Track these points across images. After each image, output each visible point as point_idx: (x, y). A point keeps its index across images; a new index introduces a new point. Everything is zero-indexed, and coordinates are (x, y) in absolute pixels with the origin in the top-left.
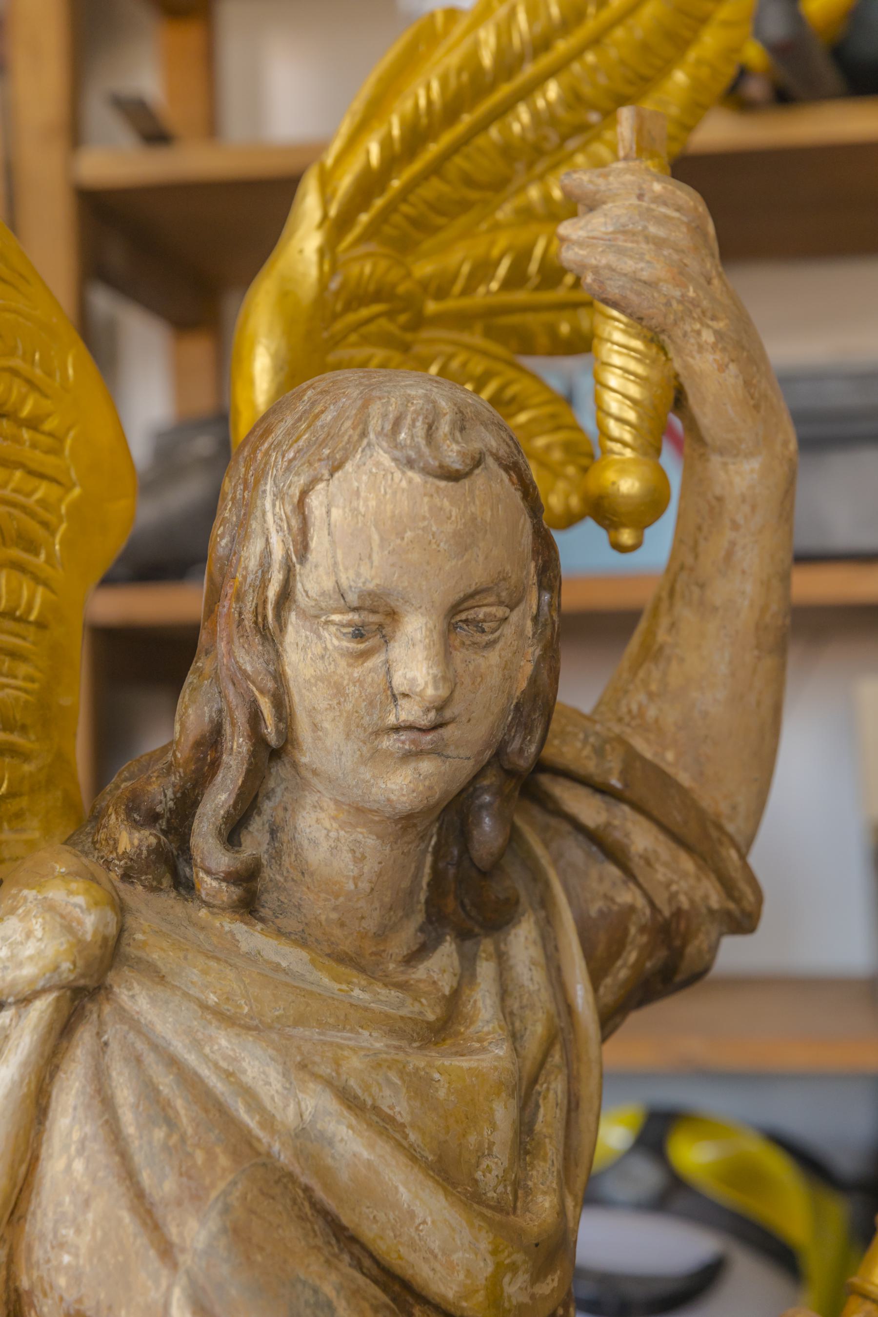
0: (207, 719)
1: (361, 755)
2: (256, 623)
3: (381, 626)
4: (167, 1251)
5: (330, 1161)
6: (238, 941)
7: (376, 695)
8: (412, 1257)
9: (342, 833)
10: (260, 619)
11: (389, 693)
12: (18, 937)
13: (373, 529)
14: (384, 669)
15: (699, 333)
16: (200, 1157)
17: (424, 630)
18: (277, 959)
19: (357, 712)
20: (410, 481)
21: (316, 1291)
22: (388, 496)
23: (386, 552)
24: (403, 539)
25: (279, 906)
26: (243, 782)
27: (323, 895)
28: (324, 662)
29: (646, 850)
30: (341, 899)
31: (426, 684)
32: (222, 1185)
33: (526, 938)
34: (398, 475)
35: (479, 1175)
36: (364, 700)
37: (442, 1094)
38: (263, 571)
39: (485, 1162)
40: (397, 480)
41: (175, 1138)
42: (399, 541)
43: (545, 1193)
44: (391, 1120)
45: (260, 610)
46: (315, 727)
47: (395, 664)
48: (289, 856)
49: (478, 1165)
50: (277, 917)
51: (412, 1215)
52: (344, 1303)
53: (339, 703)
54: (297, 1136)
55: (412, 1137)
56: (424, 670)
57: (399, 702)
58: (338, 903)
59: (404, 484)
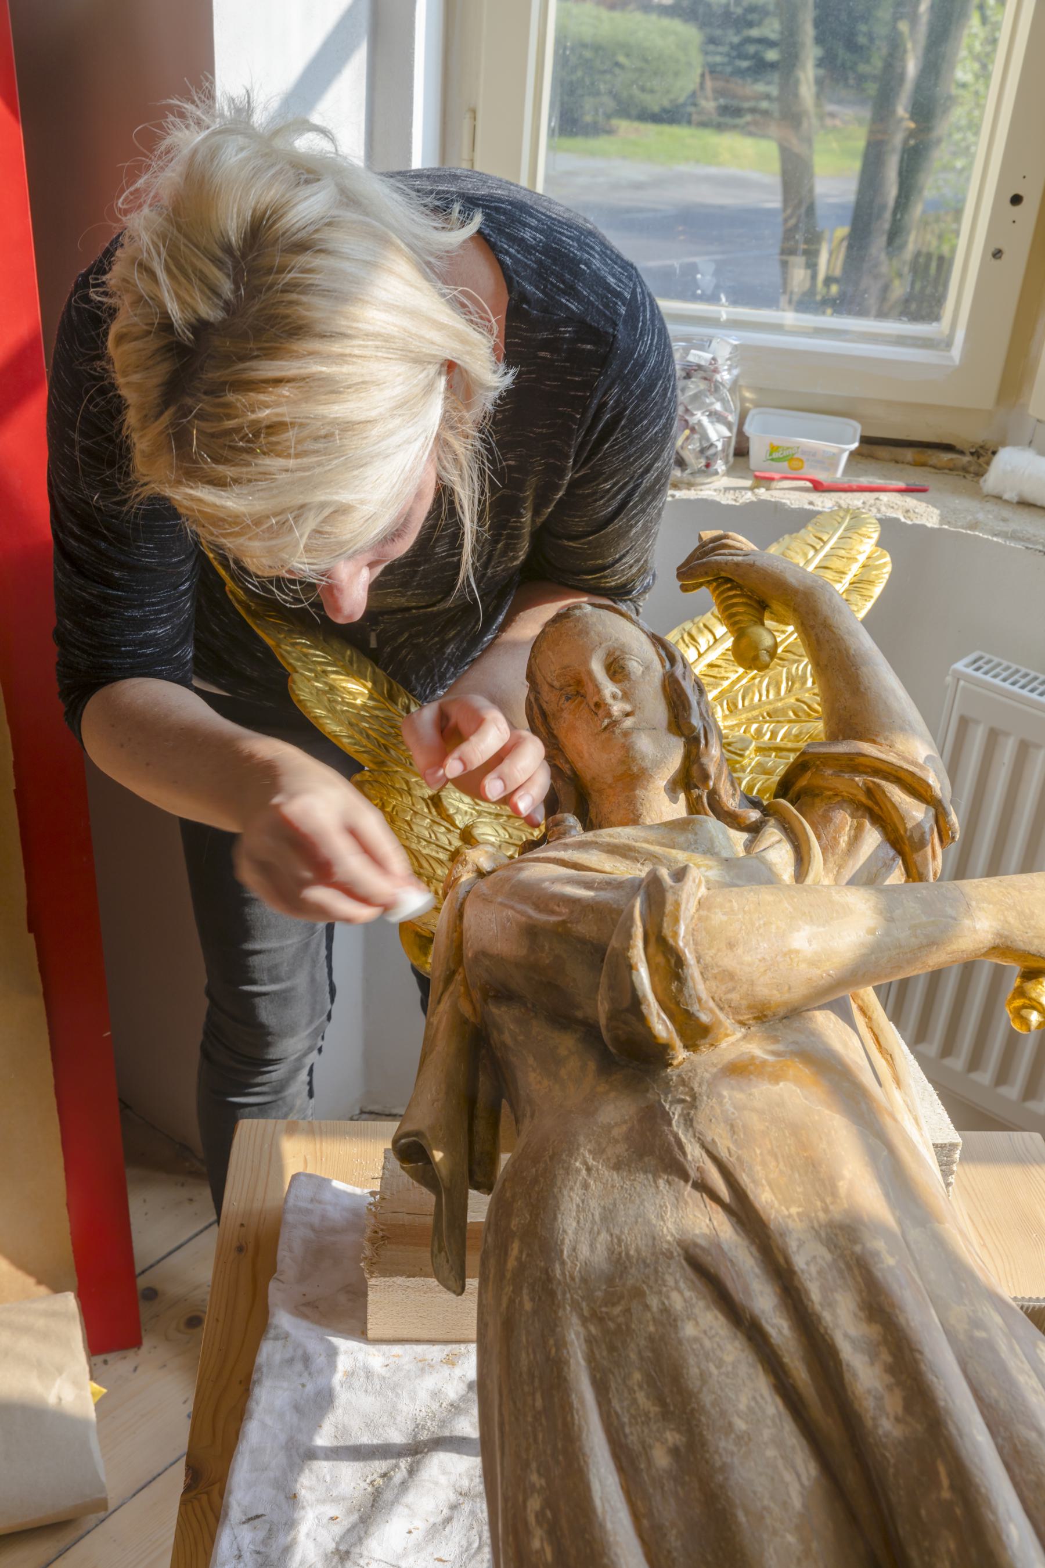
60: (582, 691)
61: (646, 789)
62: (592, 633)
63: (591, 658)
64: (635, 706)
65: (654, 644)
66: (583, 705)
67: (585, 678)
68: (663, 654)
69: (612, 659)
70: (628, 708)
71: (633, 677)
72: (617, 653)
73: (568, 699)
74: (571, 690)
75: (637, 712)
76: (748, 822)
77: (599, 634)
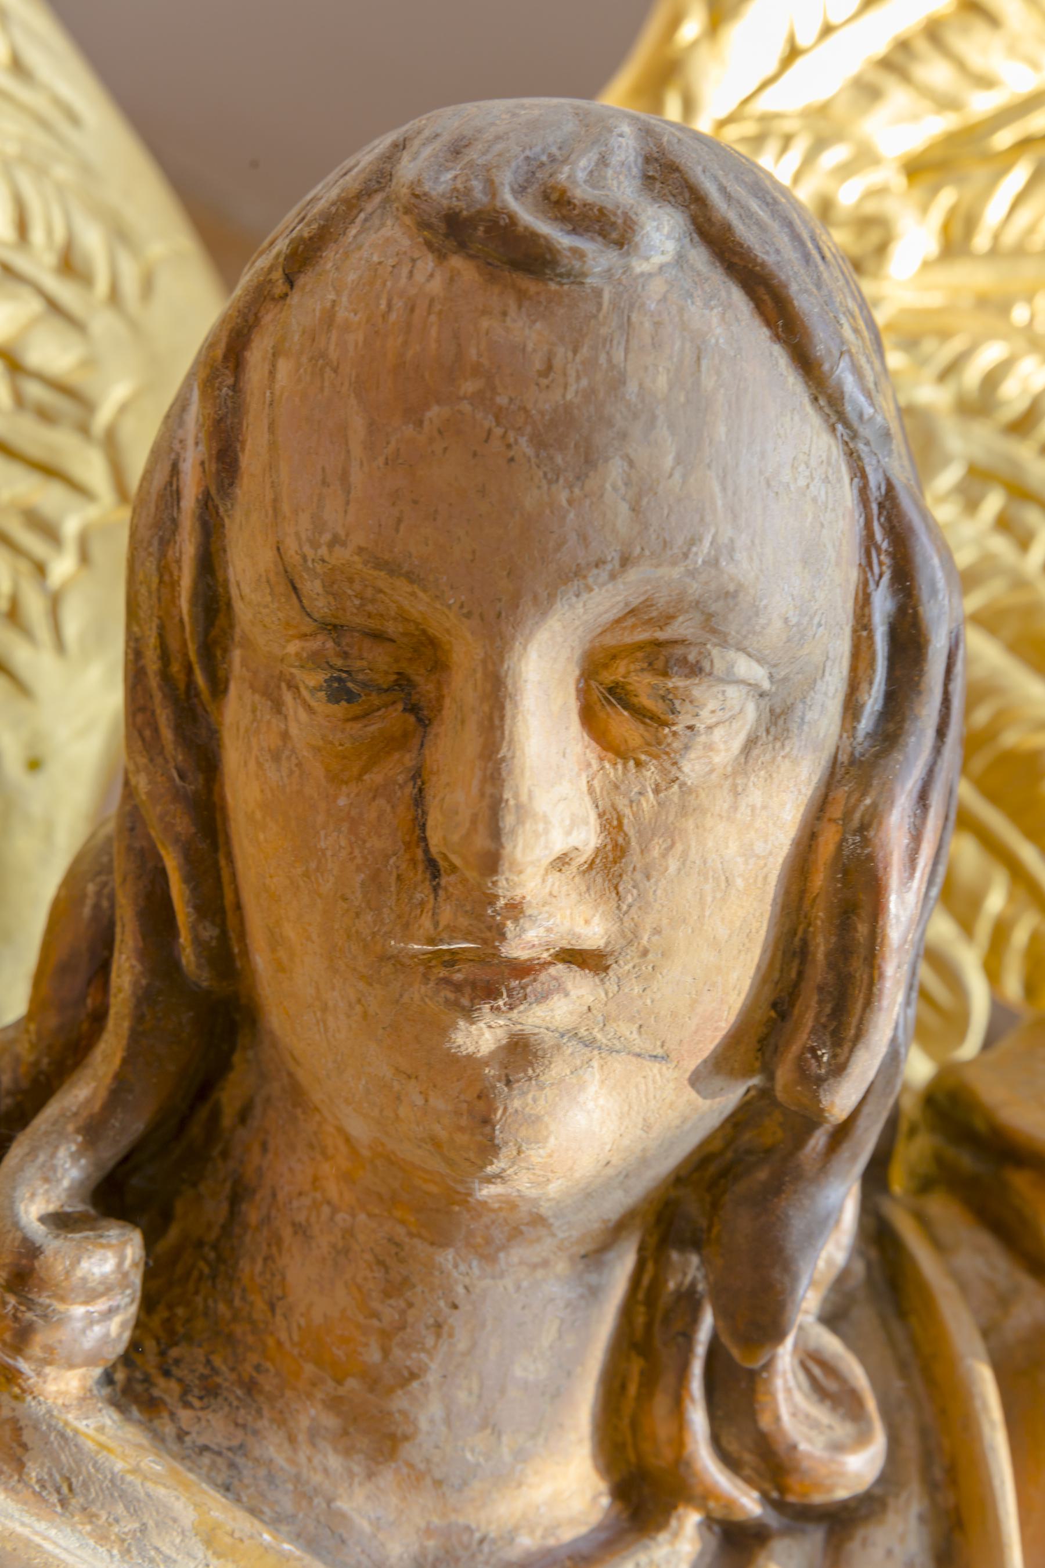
0: (87, 911)
1: (365, 1015)
2: (165, 676)
3: (403, 684)
6: (24, 1447)
7: (387, 857)
9: (362, 1217)
10: (175, 668)
11: (420, 854)
13: (353, 401)
14: (410, 790)
17: (479, 675)
19: (345, 899)
20: (452, 278)
22: (393, 317)
23: (381, 460)
24: (420, 423)
25: (203, 1377)
26: (125, 1061)
27: (309, 1369)
28: (279, 770)
30: (352, 1383)
31: (474, 821)
33: (889, 1553)
36: (358, 869)
38: (161, 539)
40: (420, 277)
42: (409, 430)
45: (174, 645)
46: (275, 941)
47: (434, 779)
48: (253, 1260)
50: (187, 1405)
53: (306, 875)
56: (475, 790)
57: (444, 881)
58: (341, 1391)
59: (436, 286)
60: (426, 687)
61: (489, 1259)
62: (615, 470)
63: (544, 607)
64: (631, 937)
65: (869, 543)
66: (394, 768)
67: (463, 688)
68: (882, 605)
69: (642, 635)
70: (593, 930)
71: (691, 768)
72: (681, 628)
73: (339, 691)
74: (377, 662)
75: (623, 967)
76: (818, 1498)
77: (641, 494)
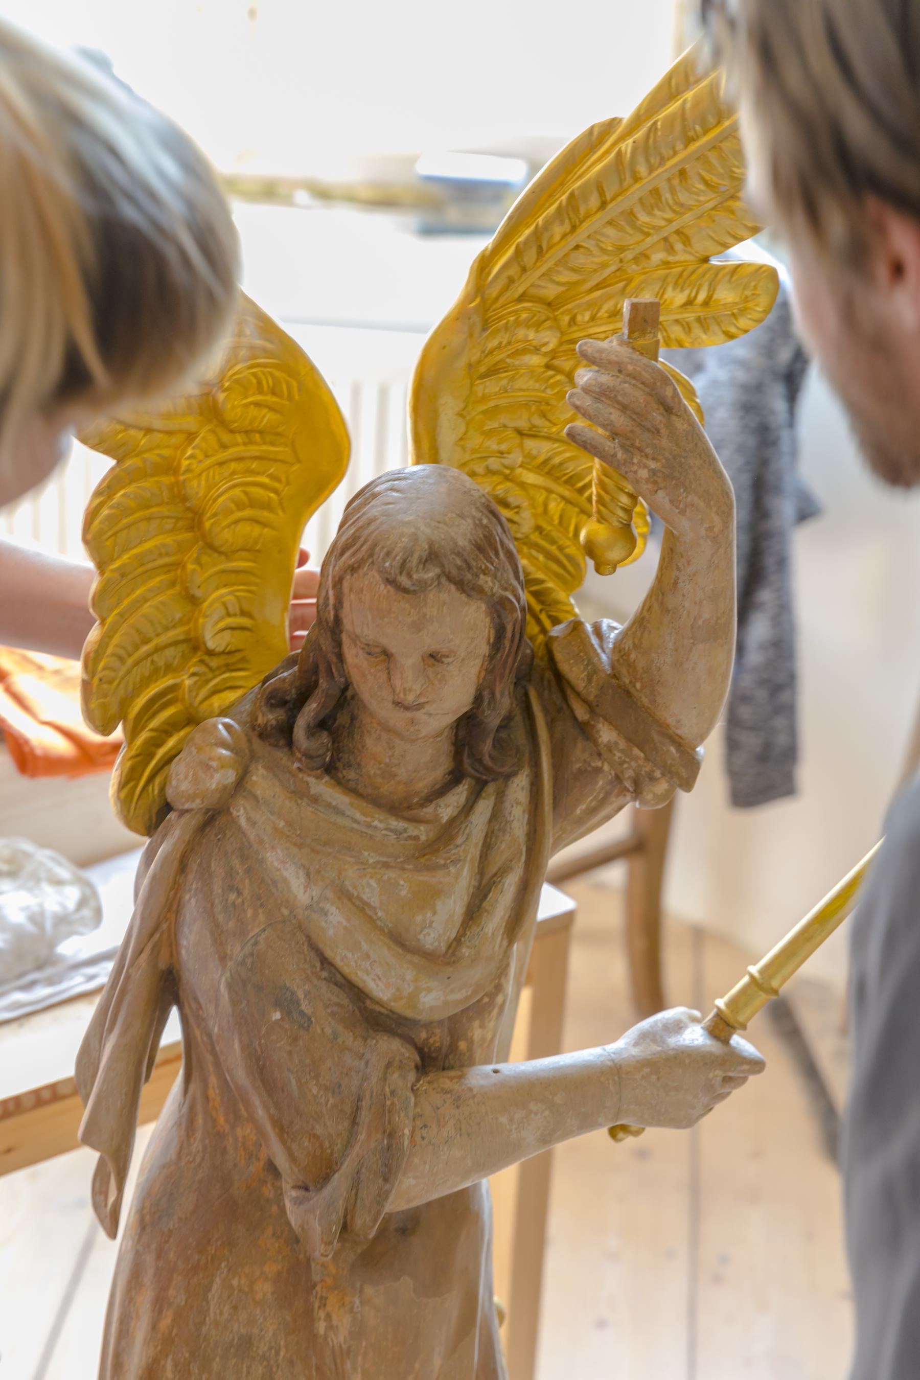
4: (223, 958)
5: (323, 924)
8: (365, 977)
12: (182, 777)
15: (636, 472)
16: (250, 913)
18: (330, 800)
20: (388, 591)
21: (293, 994)
29: (609, 741)
32: (256, 930)
34: (382, 587)
35: (421, 936)
37: (403, 893)
39: (426, 931)
41: (240, 900)
43: (468, 947)
44: (368, 905)
49: (421, 932)
51: (368, 956)
52: (307, 1002)
54: (306, 908)
55: (380, 914)
59: (385, 592)
